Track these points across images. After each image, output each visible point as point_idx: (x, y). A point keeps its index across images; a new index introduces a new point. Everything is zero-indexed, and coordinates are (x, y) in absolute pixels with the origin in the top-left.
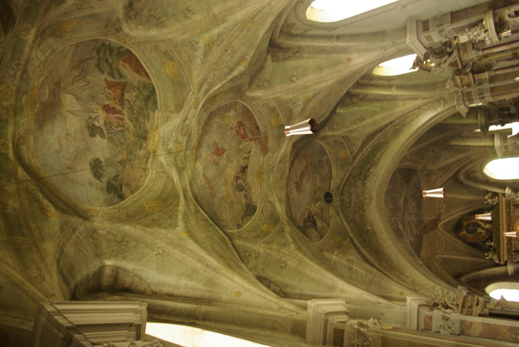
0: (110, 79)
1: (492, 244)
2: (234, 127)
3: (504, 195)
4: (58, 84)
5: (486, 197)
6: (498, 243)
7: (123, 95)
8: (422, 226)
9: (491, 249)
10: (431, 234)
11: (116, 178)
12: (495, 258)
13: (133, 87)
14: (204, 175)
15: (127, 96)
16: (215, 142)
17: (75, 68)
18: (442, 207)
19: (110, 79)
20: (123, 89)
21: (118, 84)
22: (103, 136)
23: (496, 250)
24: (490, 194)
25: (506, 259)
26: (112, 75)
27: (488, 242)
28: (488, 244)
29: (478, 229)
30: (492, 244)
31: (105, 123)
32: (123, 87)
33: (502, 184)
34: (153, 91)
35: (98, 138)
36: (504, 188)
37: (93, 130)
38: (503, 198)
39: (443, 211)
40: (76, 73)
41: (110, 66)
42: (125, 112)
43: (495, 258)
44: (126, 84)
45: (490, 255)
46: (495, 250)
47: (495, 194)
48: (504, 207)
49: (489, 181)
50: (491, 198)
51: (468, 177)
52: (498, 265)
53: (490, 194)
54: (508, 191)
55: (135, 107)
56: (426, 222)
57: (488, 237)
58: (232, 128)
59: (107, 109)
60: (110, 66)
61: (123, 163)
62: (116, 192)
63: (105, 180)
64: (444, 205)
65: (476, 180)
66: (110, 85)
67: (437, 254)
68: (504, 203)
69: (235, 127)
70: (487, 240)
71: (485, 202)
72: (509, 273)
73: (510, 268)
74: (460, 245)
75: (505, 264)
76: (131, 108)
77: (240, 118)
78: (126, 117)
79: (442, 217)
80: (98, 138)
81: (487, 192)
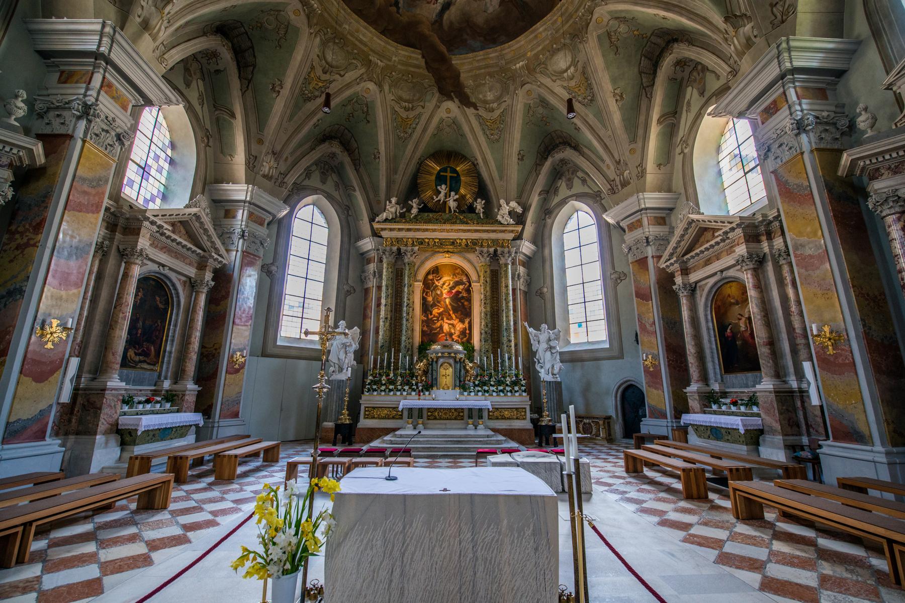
1: (414, 211)
3: (519, 237)
5: (513, 204)
6: (416, 220)
8: (443, 48)
9: (405, 210)
10: (429, 80)
12: (384, 215)
18: (492, 110)
23: (402, 217)
24: (519, 210)
25: (384, 234)
27: (419, 204)
28: (414, 203)
29: (443, 186)
30: (414, 211)
33: (541, 239)
36: (534, 241)
38: (510, 236)
39: (481, 112)
43: (384, 215)
45: (392, 208)
46: (402, 216)
47: (520, 219)
48: (493, 236)
49: (547, 212)
50: (511, 213)
51: (557, 174)
52: (372, 220)
53: (519, 210)
54: (526, 247)
56: (456, 61)
57: (429, 205)
64: (497, 113)
65: (549, 191)
67: (380, 85)
68: (500, 236)
70: (421, 202)
71: (502, 202)
72: (360, 243)
73: (367, 244)
74: (411, 153)
75: (375, 234)
79: (470, 111)
81: (526, 209)
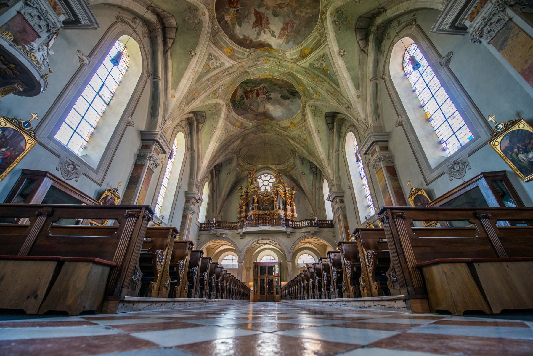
0: (245, 98)
2: (235, 10)
4: (257, 115)
7: (249, 91)
11: (288, 91)
13: (244, 89)
14: (279, 37)
15: (249, 90)
16: (253, 27)
17: (248, 111)
19: (245, 98)
20: (247, 92)
21: (245, 95)
22: (270, 95)
26: (243, 99)
31: (264, 94)
32: (246, 93)
34: (242, 83)
35: (271, 96)
37: (269, 99)
40: (249, 110)
41: (240, 102)
42: (256, 88)
44: (244, 93)
55: (253, 86)
58: (237, 11)
59: (258, 95)
60: (240, 102)
61: (280, 88)
62: (295, 93)
63: (290, 96)
66: (247, 97)
69: (235, 8)
76: (254, 87)
77: (227, 7)
78: (259, 88)
80: (271, 96)
